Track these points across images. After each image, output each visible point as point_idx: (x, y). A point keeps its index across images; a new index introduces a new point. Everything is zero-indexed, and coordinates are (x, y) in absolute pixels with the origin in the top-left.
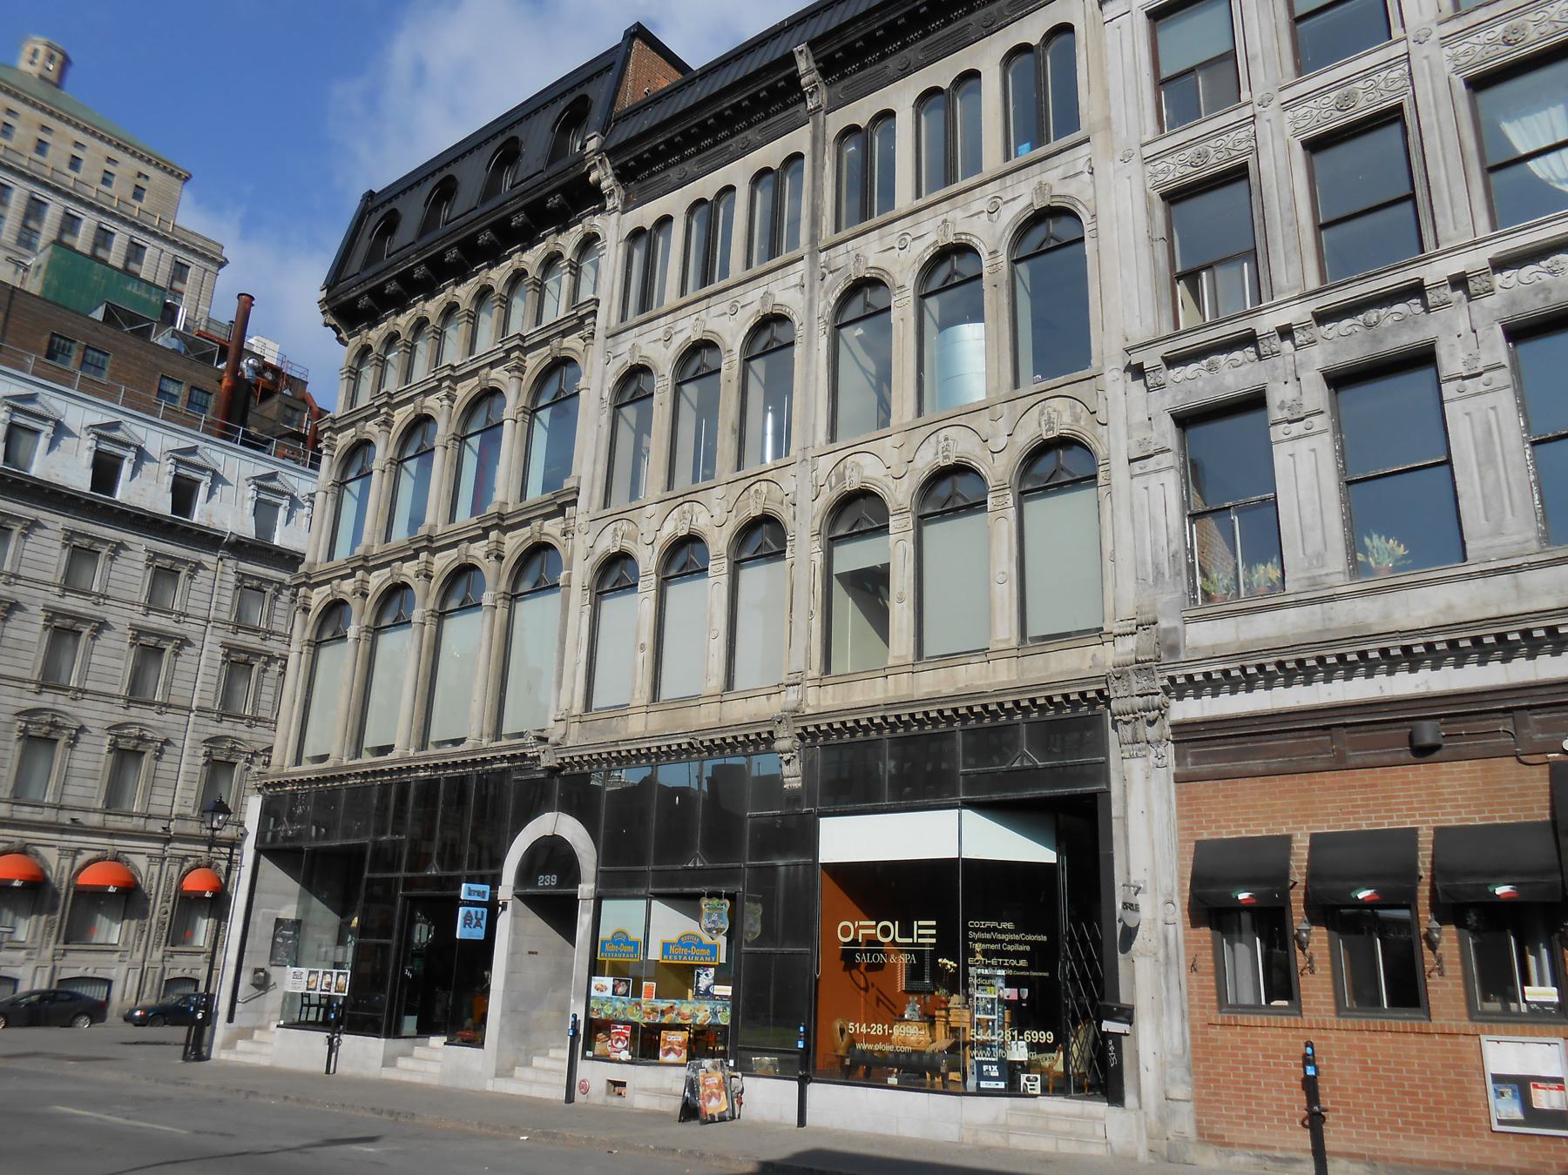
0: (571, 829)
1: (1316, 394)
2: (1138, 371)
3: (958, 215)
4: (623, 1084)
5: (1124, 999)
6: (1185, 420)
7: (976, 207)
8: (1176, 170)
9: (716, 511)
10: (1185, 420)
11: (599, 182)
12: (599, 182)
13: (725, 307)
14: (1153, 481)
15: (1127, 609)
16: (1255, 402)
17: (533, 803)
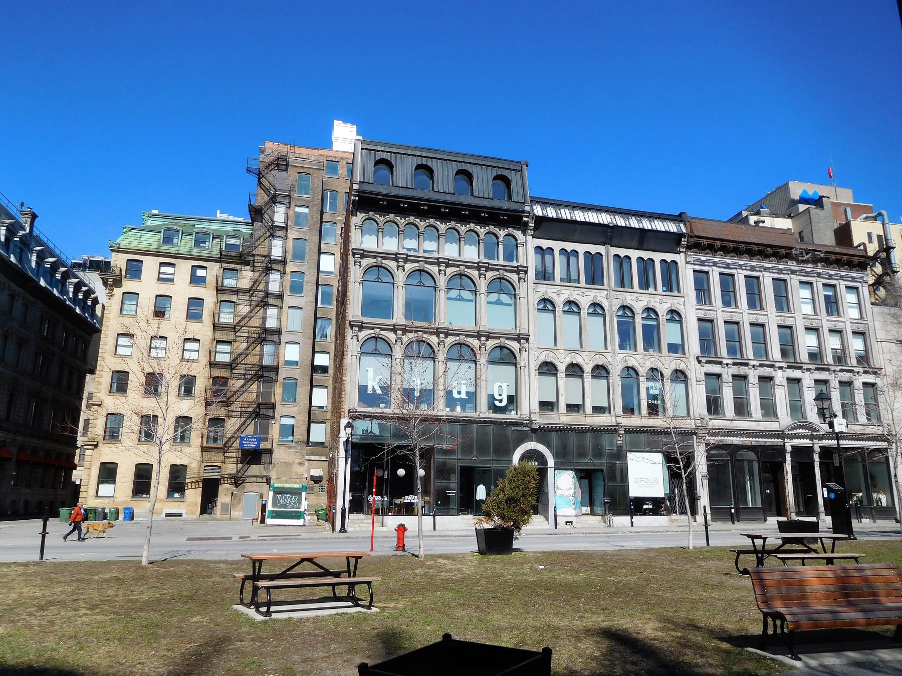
0: (541, 448)
1: (730, 379)
2: (699, 362)
3: (652, 300)
4: (571, 522)
5: (698, 495)
6: (706, 374)
7: (657, 300)
8: (701, 314)
9: (585, 359)
10: (706, 374)
11: (527, 223)
12: (527, 223)
13: (579, 293)
14: (701, 387)
15: (697, 414)
16: (719, 376)
17: (521, 439)
